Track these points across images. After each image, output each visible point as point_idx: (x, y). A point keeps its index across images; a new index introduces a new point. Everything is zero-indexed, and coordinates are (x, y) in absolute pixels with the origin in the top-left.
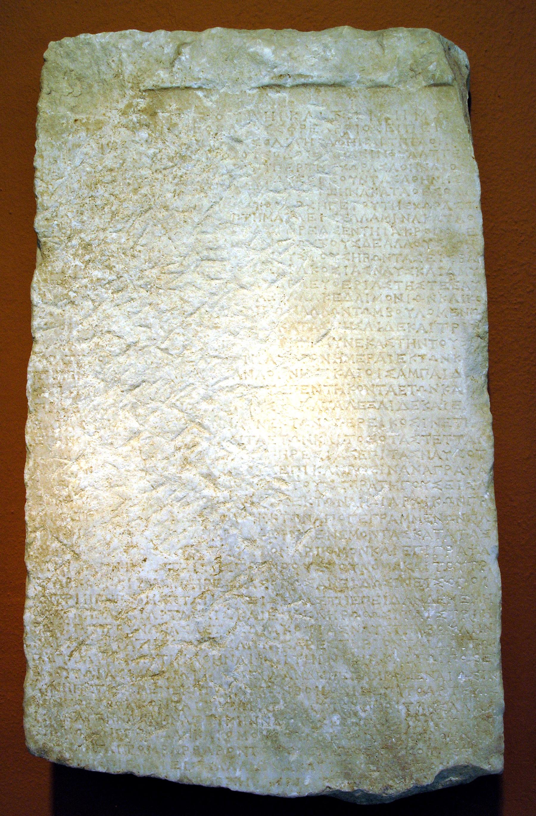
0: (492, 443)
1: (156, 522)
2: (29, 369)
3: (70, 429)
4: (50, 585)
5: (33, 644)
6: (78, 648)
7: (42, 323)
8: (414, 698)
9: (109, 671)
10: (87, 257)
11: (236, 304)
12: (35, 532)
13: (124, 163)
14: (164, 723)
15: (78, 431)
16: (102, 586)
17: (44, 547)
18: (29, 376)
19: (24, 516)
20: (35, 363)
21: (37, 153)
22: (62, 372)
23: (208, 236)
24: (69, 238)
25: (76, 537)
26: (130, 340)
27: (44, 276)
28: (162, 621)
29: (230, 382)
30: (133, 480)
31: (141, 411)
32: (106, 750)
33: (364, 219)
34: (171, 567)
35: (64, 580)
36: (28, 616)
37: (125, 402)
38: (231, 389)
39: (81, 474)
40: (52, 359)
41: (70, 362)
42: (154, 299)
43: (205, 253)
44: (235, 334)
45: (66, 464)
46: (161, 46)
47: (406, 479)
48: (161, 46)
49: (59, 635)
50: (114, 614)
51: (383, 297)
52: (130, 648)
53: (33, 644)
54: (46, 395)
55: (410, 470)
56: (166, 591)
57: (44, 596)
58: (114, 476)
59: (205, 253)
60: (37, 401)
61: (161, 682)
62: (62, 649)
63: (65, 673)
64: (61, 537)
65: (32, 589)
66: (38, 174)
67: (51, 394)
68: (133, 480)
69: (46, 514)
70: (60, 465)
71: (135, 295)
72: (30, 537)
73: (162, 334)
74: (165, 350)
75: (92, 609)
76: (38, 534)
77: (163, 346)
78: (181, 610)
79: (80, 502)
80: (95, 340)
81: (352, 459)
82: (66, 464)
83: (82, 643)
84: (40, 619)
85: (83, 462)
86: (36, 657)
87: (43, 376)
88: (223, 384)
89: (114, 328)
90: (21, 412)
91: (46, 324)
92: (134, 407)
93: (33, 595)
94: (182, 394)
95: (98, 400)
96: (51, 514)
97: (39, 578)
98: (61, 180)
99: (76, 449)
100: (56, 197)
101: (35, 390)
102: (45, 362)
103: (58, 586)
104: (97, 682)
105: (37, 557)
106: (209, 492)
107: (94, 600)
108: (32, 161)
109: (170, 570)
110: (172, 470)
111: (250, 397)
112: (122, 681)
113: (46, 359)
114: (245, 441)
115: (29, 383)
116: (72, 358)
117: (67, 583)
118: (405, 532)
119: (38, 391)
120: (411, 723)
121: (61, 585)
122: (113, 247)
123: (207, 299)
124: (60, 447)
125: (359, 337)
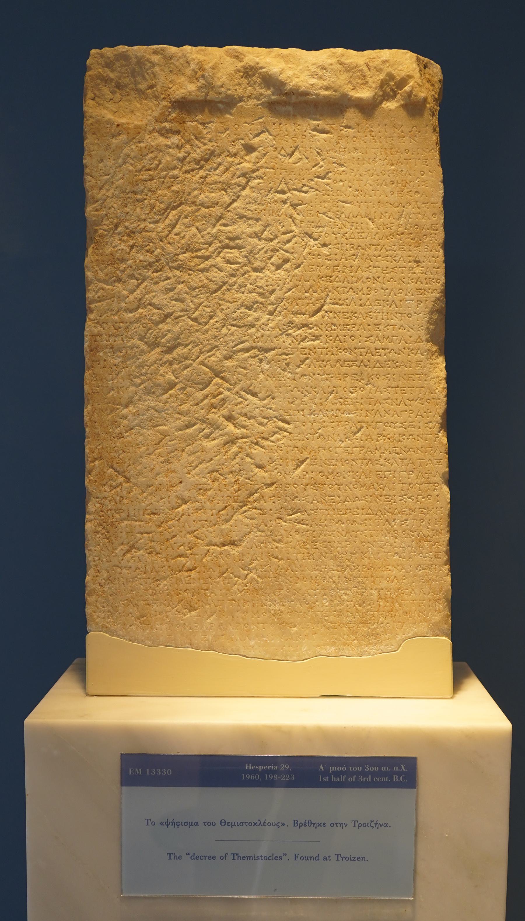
0: (445, 393)
1: (189, 453)
2: (86, 333)
3: (121, 380)
4: (107, 502)
5: (93, 548)
6: (129, 551)
7: (96, 296)
8: (384, 584)
9: (154, 567)
10: (131, 242)
11: (251, 284)
12: (94, 462)
13: (160, 164)
14: (196, 606)
15: (127, 383)
16: (147, 503)
17: (102, 473)
18: (86, 339)
19: (84, 449)
20: (90, 327)
21: (86, 153)
22: (113, 335)
23: (228, 228)
24: (116, 226)
25: (126, 465)
26: (168, 310)
27: (97, 258)
28: (194, 529)
29: (246, 345)
30: (171, 420)
31: (175, 366)
32: (152, 628)
33: (351, 215)
34: (201, 487)
35: (118, 499)
36: (89, 526)
37: (164, 360)
38: (247, 350)
39: (130, 417)
40: (104, 325)
41: (120, 328)
42: (186, 277)
43: (227, 241)
44: (250, 308)
45: (118, 409)
46: (187, 62)
47: (379, 420)
48: (187, 62)
49: (114, 540)
50: (158, 523)
51: (364, 279)
52: (170, 549)
53: (93, 548)
54: (101, 354)
55: (383, 413)
56: (197, 504)
57: (102, 511)
58: (156, 418)
59: (227, 241)
60: (93, 358)
61: (193, 574)
62: (117, 551)
63: (119, 570)
64: (115, 465)
65: (92, 506)
66: (87, 170)
67: (105, 353)
68: (171, 420)
69: (102, 448)
70: (114, 410)
71: (170, 275)
72: (88, 466)
73: (193, 306)
74: (195, 320)
75: (140, 520)
76: (97, 463)
77: (193, 316)
78: (209, 520)
79: (129, 439)
80: (140, 311)
81: (338, 405)
82: (118, 409)
83: (132, 547)
84: (99, 529)
85: (131, 408)
86: (97, 558)
87: (98, 339)
88: (240, 346)
89: (155, 301)
90: (79, 367)
91: (99, 297)
92: (171, 364)
93: (93, 510)
94: (209, 354)
95: (143, 358)
96: (107, 447)
97: (97, 498)
98: (107, 177)
99: (125, 396)
100: (103, 191)
101: (91, 350)
102: (99, 328)
103: (113, 503)
104: (144, 576)
105: (96, 481)
106: (231, 428)
107: (141, 513)
108: (82, 159)
109: (200, 489)
110: (202, 413)
111: (261, 356)
112: (164, 575)
113: (101, 325)
114: (257, 390)
115: (86, 345)
116: (121, 324)
117: (120, 501)
118: (378, 460)
119: (94, 350)
120: (381, 603)
121: (116, 502)
122: (153, 235)
123: (227, 279)
124: (113, 395)
125: (346, 310)
